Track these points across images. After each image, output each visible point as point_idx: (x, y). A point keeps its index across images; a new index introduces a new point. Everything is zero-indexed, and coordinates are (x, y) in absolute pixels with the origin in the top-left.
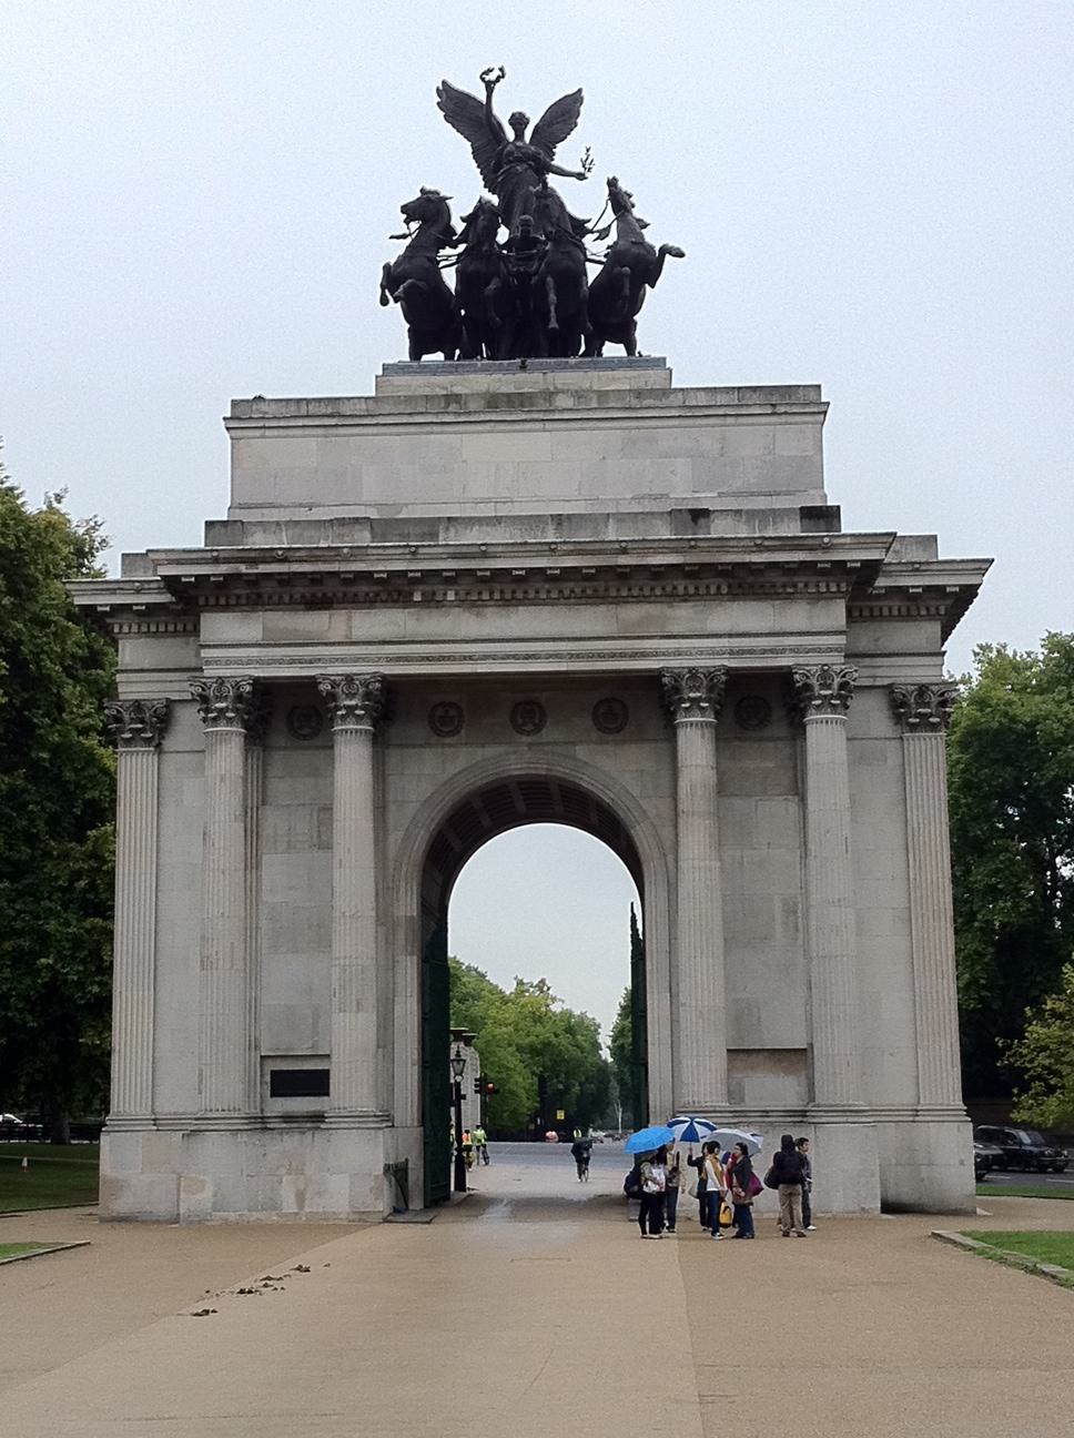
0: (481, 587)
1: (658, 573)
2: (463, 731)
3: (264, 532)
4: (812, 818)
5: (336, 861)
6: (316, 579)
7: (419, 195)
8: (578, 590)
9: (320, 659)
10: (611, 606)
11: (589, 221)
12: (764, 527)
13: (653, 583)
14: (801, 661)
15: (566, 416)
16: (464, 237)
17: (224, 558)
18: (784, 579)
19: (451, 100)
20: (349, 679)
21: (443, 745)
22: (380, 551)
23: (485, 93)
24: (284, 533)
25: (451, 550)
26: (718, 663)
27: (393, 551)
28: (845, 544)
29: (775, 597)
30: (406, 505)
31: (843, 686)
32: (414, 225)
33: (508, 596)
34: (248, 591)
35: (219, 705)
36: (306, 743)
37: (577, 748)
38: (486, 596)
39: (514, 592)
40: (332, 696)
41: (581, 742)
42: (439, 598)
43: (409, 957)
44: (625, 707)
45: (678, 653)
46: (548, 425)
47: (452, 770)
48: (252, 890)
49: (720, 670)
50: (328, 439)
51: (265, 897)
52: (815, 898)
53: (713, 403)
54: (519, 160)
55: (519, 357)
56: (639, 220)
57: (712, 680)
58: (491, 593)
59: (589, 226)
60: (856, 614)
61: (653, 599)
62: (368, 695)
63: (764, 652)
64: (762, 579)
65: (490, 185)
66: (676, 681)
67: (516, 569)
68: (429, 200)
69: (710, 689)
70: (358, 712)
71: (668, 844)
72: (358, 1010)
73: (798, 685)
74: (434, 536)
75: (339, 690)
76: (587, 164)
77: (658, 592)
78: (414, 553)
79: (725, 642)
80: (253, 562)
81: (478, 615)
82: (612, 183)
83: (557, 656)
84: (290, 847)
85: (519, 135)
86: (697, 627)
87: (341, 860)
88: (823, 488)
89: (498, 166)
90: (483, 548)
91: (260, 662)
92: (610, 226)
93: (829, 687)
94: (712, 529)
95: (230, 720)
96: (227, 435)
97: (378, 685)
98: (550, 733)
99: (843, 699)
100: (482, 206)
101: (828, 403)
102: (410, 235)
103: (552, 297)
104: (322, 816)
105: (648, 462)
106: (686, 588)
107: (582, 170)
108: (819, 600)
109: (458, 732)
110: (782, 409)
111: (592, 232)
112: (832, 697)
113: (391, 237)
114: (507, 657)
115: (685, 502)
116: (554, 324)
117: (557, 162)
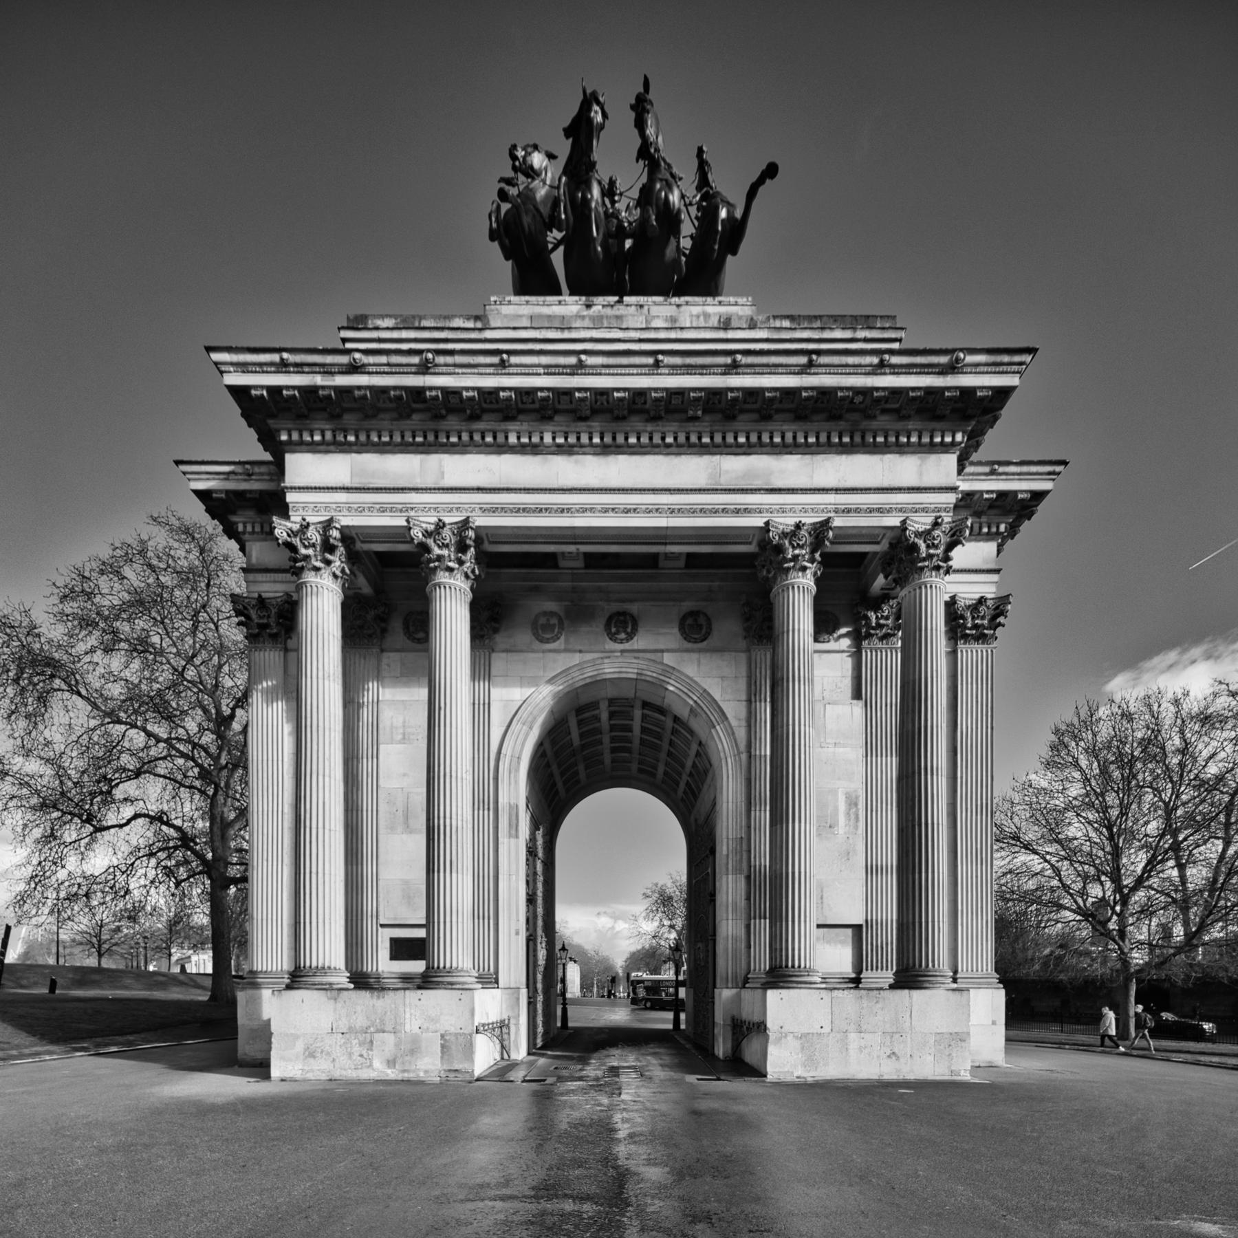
2: (563, 638)
21: (544, 652)
37: (665, 654)
41: (668, 651)
98: (641, 641)
109: (558, 638)
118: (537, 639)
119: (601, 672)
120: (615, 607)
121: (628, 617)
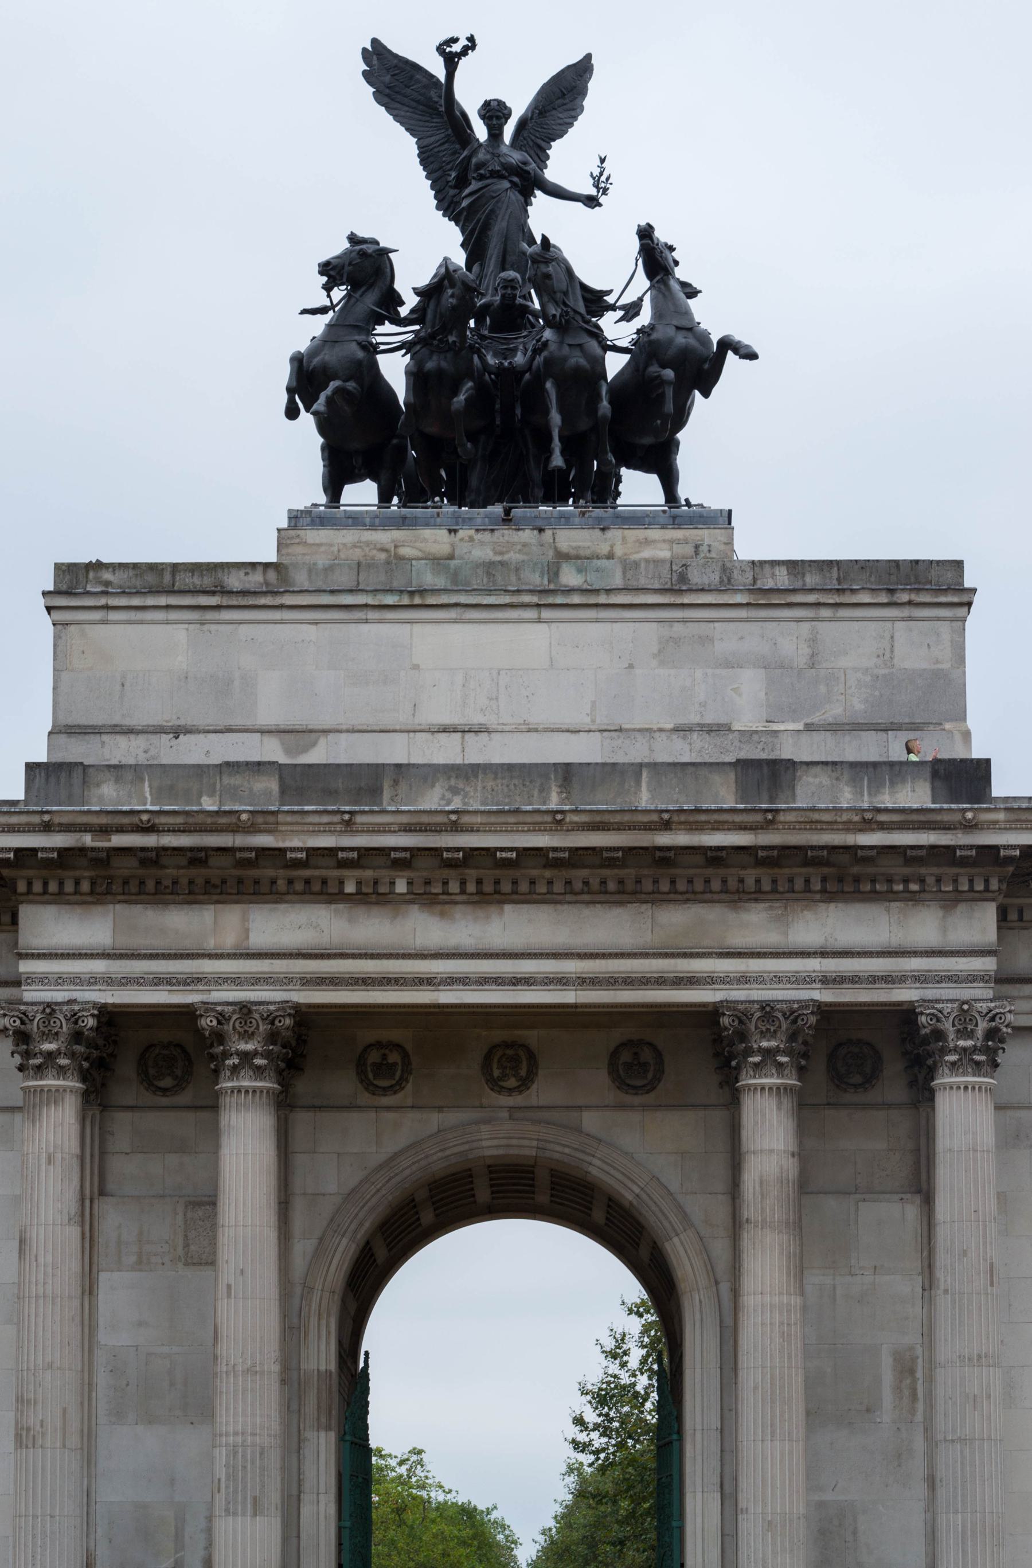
0: (446, 872)
1: (716, 857)
2: (409, 1087)
3: (117, 780)
4: (942, 1234)
5: (222, 1288)
6: (198, 857)
7: (347, 245)
8: (595, 883)
9: (199, 980)
10: (644, 906)
11: (609, 292)
12: (876, 787)
13: (709, 871)
14: (930, 993)
15: (576, 599)
16: (418, 315)
17: (60, 825)
18: (907, 871)
19: (388, 70)
20: (245, 1009)
21: (377, 1108)
22: (297, 818)
23: (444, 72)
24: (147, 784)
25: (404, 819)
26: (804, 995)
27: (315, 819)
28: (996, 822)
29: (891, 896)
30: (326, 732)
31: (992, 1034)
32: (338, 294)
33: (488, 888)
34: (93, 873)
35: (49, 1046)
36: (165, 1101)
38: (454, 887)
39: (497, 882)
40: (220, 1037)
41: (588, 1107)
42: (383, 889)
43: (323, 1434)
44: (659, 1055)
45: (744, 979)
46: (546, 614)
47: (390, 1147)
48: (89, 1323)
49: (807, 1007)
50: (206, 627)
51: (104, 1337)
52: (944, 1352)
53: (798, 585)
54: (496, 175)
55: (500, 500)
56: (684, 285)
57: (795, 1021)
58: (463, 883)
59: (610, 299)
60: (1013, 916)
61: (708, 896)
62: (272, 1037)
63: (874, 979)
64: (870, 870)
65: (448, 206)
66: (741, 1022)
67: (502, 849)
68: (363, 254)
69: (792, 1037)
70: (259, 1061)
71: (722, 1265)
72: (255, 1515)
73: (923, 1032)
74: (374, 792)
75: (228, 1028)
76: (601, 183)
77: (716, 885)
78: (348, 823)
79: (814, 965)
80: (104, 831)
81: (442, 915)
82: (646, 233)
83: (561, 981)
84: (141, 1263)
85: (495, 134)
86: (771, 938)
87: (229, 1286)
88: (964, 719)
89: (462, 182)
90: (453, 817)
91: (108, 981)
92: (641, 299)
93: (970, 1035)
94: (799, 790)
95: (62, 1071)
96: (46, 620)
97: (288, 1021)
99: (992, 1054)
100: (446, 277)
101: (974, 591)
102: (333, 307)
103: (556, 418)
104: (189, 1215)
105: (699, 674)
106: (758, 881)
107: (593, 192)
108: (958, 901)
109: (403, 1089)
110: (905, 597)
111: (613, 308)
112: (975, 1049)
113: (305, 312)
114: (484, 981)
115: (755, 737)
116: (557, 461)
117: (551, 174)
118: (367, 1089)
119: (475, 1145)
120: (499, 1035)
121: (521, 1053)
